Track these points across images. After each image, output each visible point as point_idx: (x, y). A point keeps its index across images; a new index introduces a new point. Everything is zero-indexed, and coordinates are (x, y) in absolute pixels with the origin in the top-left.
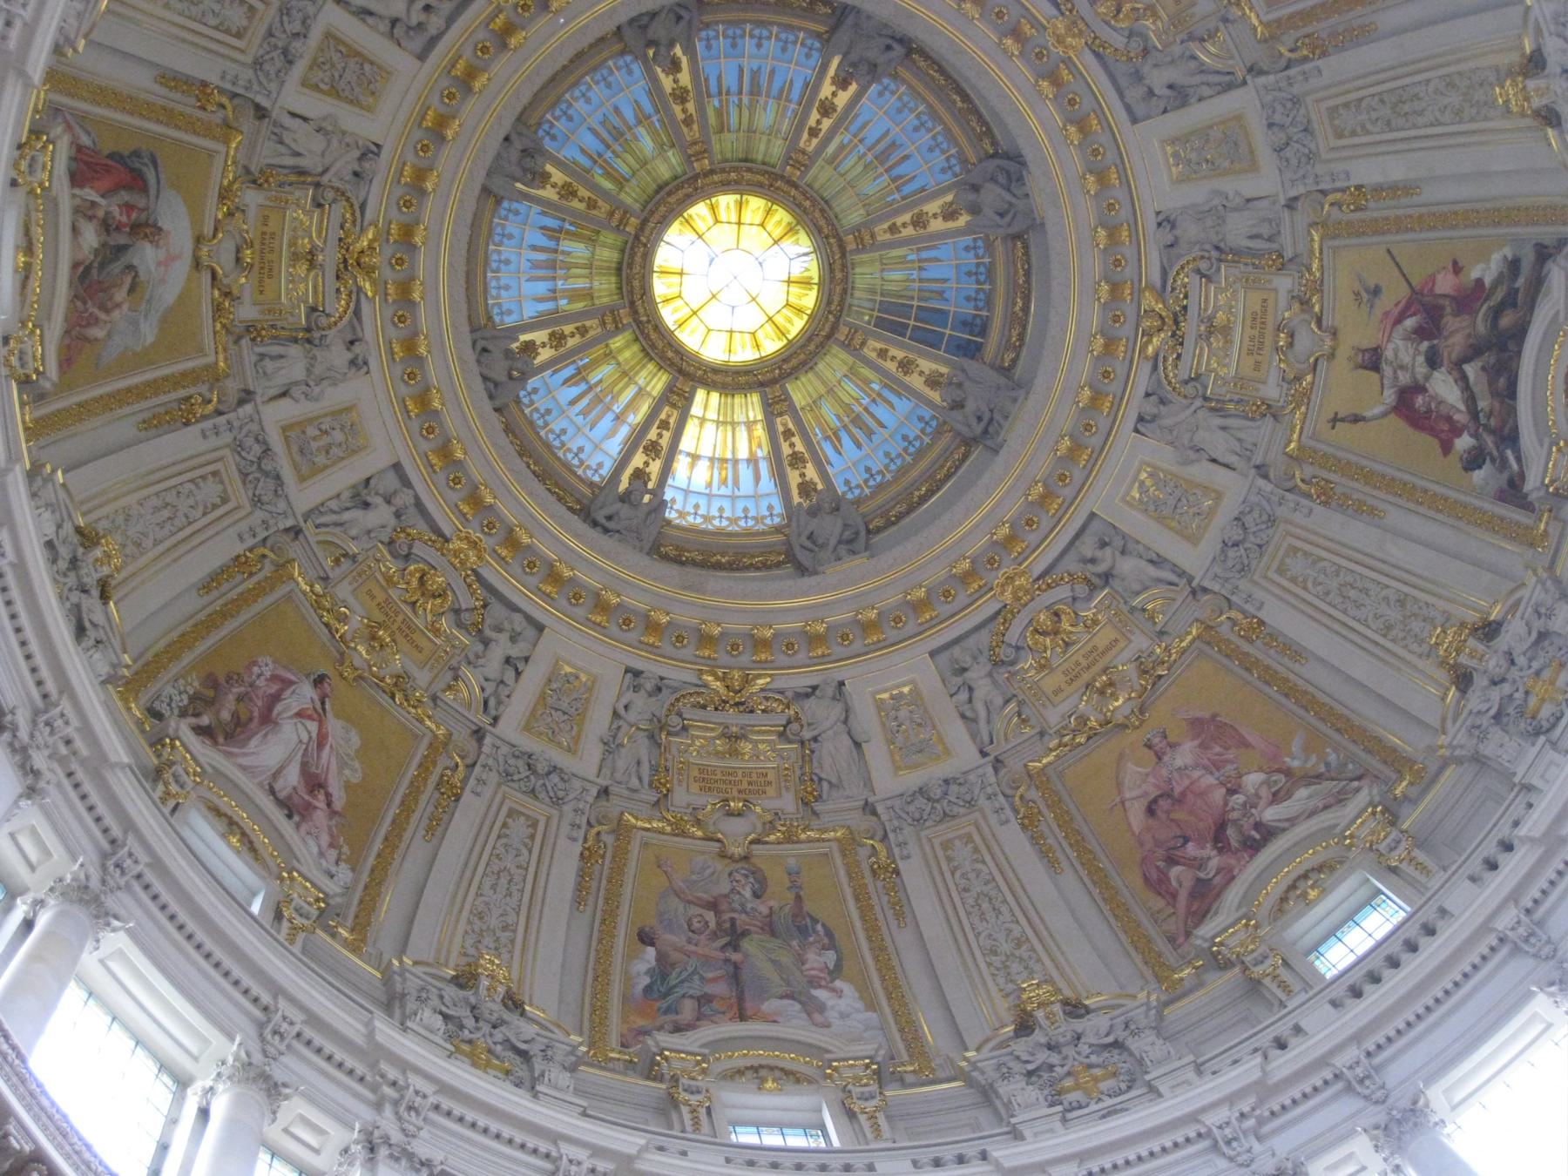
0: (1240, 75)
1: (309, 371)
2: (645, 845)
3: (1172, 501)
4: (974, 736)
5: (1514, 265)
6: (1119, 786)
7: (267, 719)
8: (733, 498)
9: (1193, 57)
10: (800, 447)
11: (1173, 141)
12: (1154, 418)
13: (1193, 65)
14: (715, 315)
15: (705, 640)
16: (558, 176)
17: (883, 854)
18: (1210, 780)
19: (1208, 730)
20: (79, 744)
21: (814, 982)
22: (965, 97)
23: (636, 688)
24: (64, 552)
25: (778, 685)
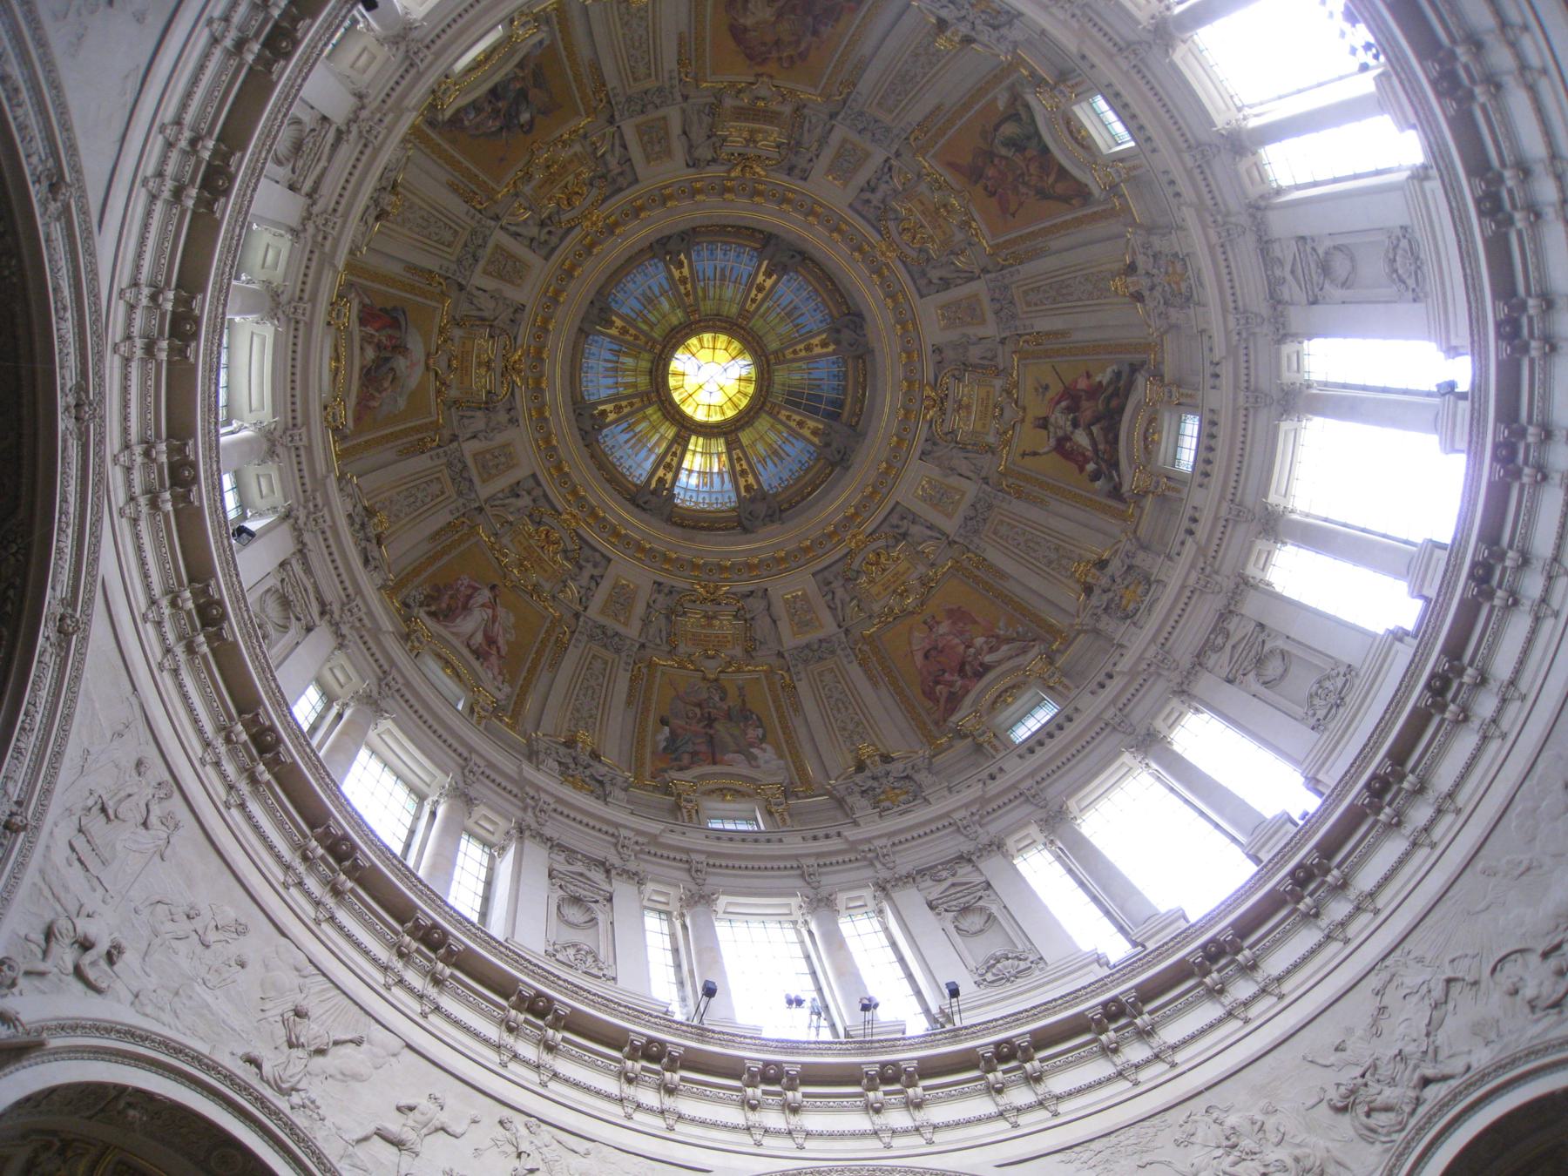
0: (977, 271)
1: (487, 425)
2: (663, 673)
3: (938, 496)
4: (835, 617)
5: (1118, 374)
6: (910, 644)
7: (466, 608)
8: (710, 493)
9: (953, 263)
10: (745, 466)
11: (942, 308)
12: (930, 453)
13: (952, 267)
14: (701, 396)
15: (695, 566)
16: (619, 323)
17: (787, 678)
18: (957, 641)
19: (958, 615)
20: (366, 621)
21: (752, 745)
22: (833, 283)
24: (357, 520)
25: (734, 590)
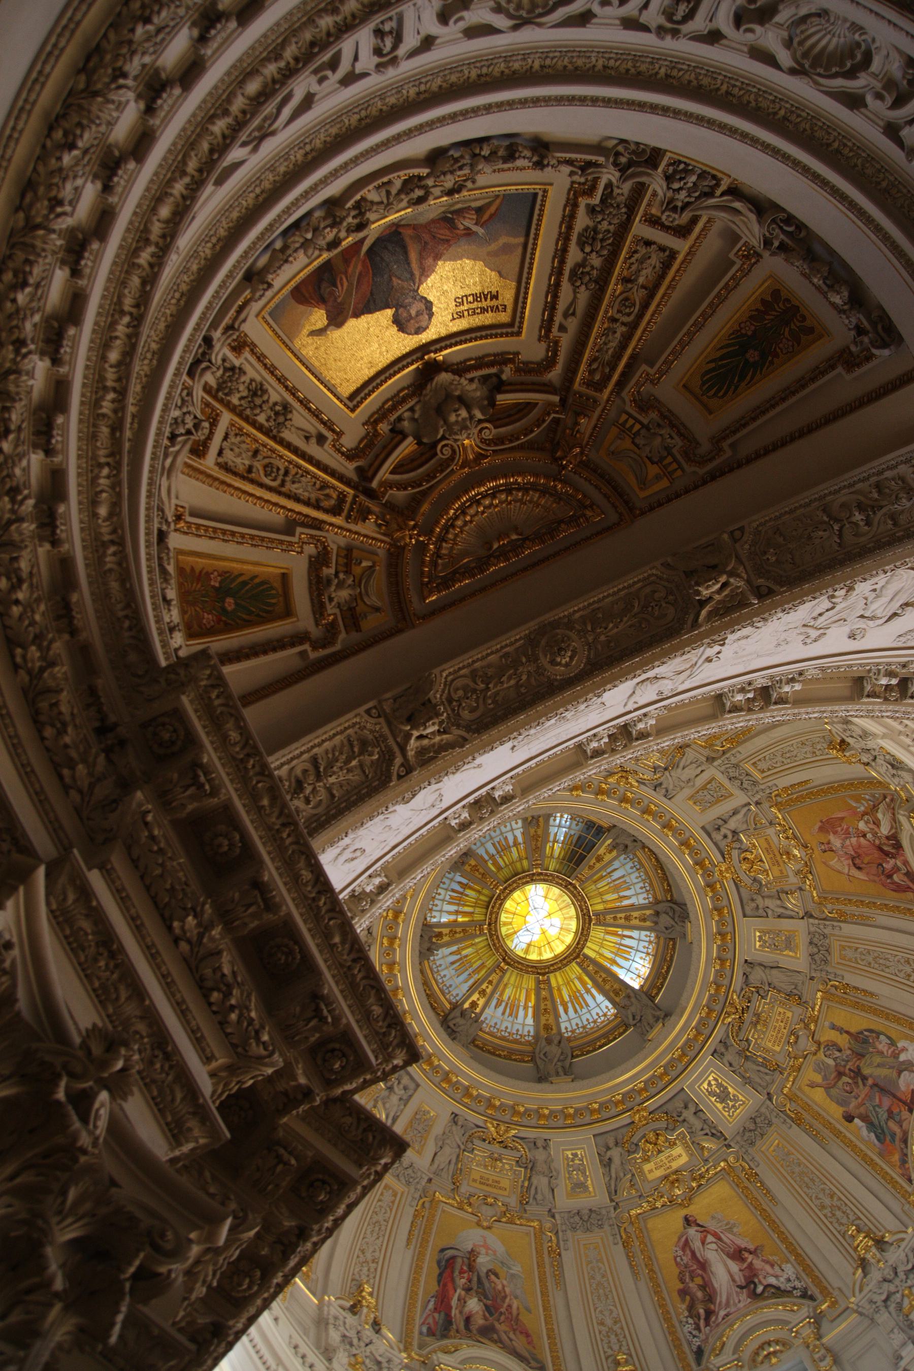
4: (792, 917)
6: (839, 872)
7: (703, 1265)
14: (553, 932)
18: (854, 840)
21: (896, 1056)
23: (722, 1054)
25: (738, 991)
